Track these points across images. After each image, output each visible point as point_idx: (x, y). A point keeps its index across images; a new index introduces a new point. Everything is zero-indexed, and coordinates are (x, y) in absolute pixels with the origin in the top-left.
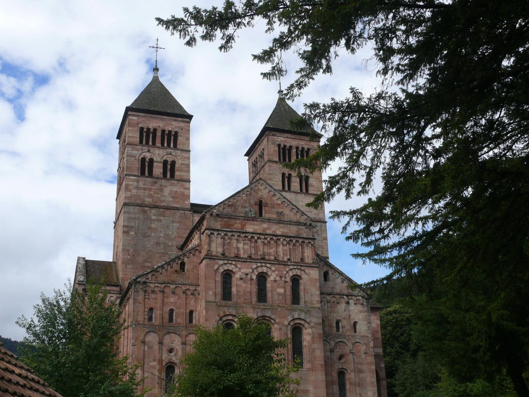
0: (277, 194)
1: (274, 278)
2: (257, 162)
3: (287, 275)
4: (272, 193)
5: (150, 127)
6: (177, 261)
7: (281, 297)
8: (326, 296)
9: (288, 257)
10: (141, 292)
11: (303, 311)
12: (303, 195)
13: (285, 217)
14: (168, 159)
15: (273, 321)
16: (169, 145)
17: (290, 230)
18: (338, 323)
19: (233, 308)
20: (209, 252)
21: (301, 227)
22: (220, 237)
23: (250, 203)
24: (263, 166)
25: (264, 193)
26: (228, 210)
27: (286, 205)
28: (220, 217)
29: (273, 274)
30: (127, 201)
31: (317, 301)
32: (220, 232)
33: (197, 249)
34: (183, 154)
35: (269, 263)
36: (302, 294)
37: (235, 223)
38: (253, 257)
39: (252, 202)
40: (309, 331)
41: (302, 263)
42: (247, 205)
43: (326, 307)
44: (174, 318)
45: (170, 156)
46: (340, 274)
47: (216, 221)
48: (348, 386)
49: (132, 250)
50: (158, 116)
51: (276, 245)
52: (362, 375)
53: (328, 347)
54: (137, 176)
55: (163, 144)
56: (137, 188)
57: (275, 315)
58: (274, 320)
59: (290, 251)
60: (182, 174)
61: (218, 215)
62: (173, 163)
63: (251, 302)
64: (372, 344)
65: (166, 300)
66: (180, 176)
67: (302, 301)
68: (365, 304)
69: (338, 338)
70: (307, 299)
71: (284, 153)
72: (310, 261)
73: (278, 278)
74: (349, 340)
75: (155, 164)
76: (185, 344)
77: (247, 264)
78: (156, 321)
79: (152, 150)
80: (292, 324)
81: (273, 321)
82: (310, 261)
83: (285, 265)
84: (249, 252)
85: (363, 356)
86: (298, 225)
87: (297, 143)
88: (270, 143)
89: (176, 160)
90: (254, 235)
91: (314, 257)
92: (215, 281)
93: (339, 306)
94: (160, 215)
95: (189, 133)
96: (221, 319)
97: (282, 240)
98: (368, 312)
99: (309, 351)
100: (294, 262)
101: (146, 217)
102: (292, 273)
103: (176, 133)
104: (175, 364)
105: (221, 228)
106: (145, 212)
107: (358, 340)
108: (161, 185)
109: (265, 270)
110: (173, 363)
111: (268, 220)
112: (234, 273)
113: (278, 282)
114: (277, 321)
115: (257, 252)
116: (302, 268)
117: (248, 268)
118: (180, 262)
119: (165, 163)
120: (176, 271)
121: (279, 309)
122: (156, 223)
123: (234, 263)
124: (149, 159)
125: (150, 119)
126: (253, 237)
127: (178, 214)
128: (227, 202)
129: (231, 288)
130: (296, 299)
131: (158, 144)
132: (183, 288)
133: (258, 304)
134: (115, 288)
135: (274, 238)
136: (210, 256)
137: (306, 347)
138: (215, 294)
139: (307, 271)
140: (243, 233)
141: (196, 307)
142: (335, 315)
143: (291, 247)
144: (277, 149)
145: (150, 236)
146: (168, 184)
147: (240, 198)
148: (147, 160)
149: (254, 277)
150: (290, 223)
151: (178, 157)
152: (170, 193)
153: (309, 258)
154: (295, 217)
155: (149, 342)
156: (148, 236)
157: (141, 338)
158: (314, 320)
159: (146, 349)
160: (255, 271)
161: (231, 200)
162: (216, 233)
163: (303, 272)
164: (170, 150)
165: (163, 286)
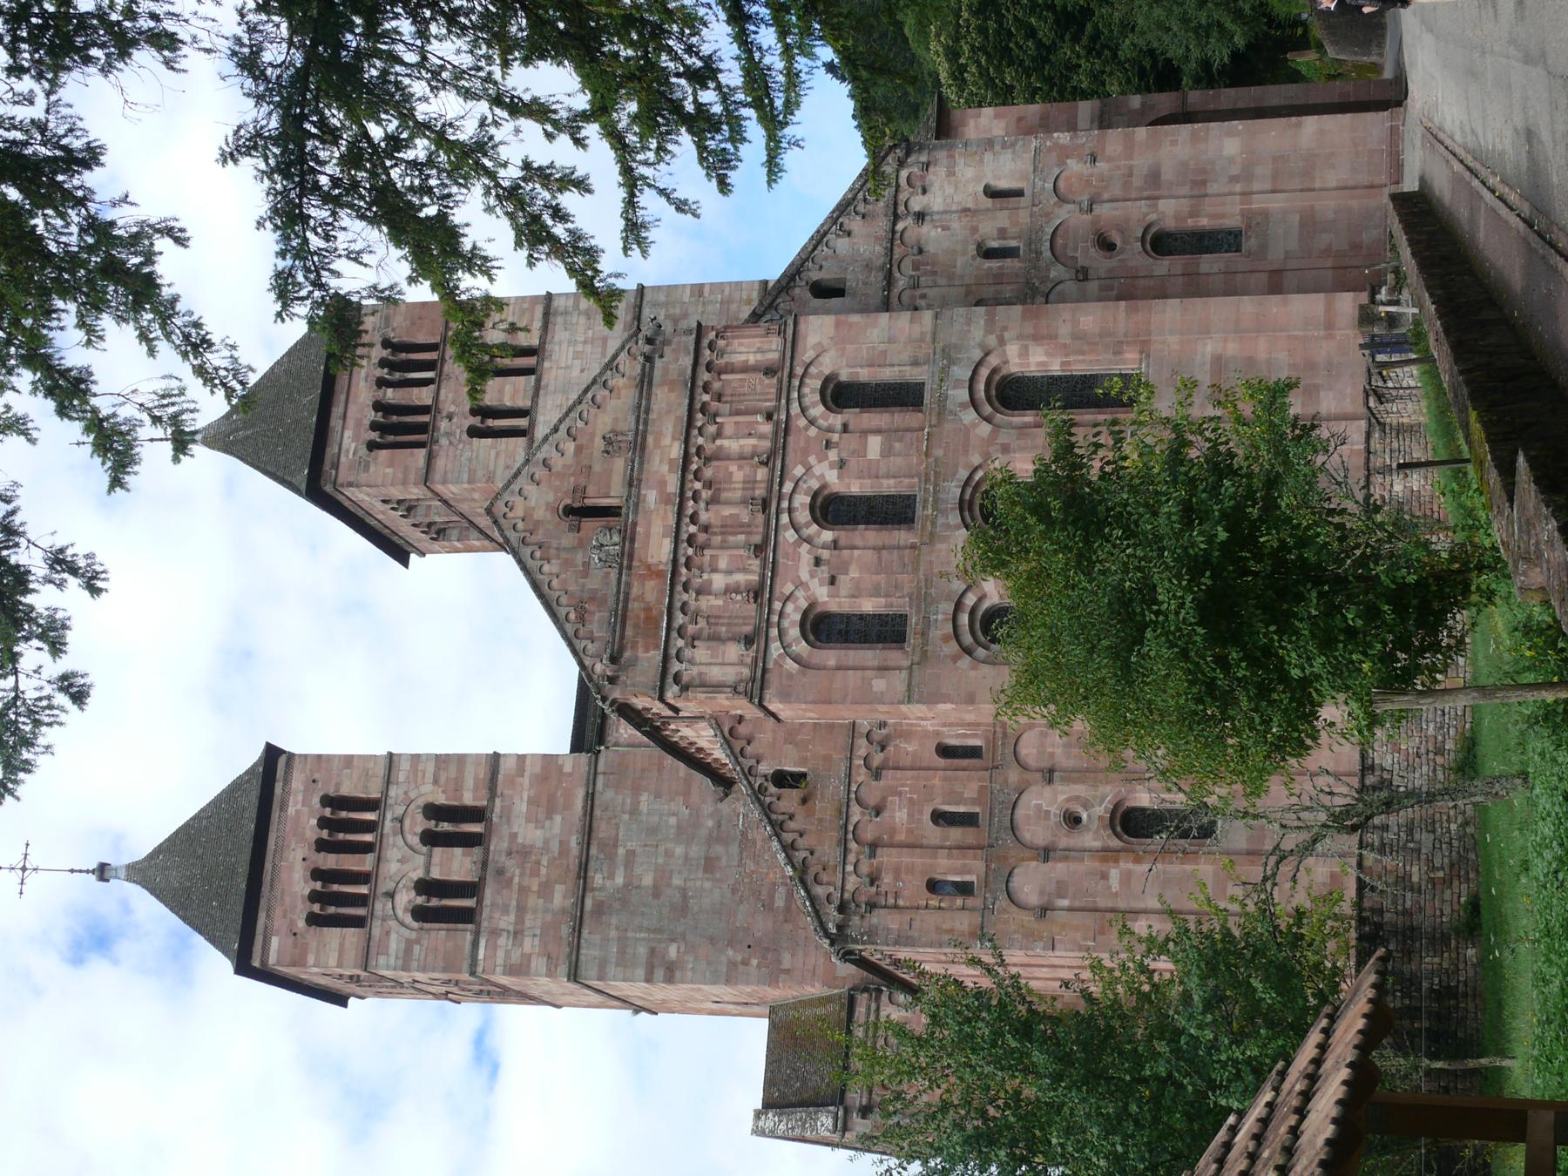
0: (540, 456)
1: (831, 467)
2: (430, 525)
3: (821, 422)
4: (540, 473)
5: (307, 892)
6: (768, 800)
7: (897, 445)
8: (896, 291)
9: (759, 418)
10: (875, 920)
11: (945, 370)
12: (546, 364)
13: (622, 426)
14: (419, 830)
15: (979, 475)
16: (369, 827)
17: (668, 412)
18: (989, 254)
19: (933, 608)
20: (741, 688)
21: (657, 373)
22: (687, 653)
23: (573, 549)
24: (445, 502)
25: (538, 501)
26: (598, 623)
27: (580, 424)
28: (621, 649)
29: (817, 471)
30: (563, 969)
31: (912, 321)
32: (673, 652)
33: (731, 730)
34: (401, 778)
35: (781, 485)
36: (887, 374)
37: (641, 598)
38: (757, 539)
39: (569, 539)
40: (1012, 350)
41: (784, 374)
42: (579, 557)
43: (931, 293)
44: (962, 809)
45: (407, 823)
46: (819, 242)
47: (634, 662)
48: (1204, 223)
49: (730, 952)
50: (268, 866)
51: (718, 459)
52: (1167, 174)
53: (1070, 287)
54: (477, 935)
55: (366, 848)
56: (517, 934)
57: (956, 466)
58: (975, 470)
59: (738, 413)
60: (469, 782)
61: (614, 659)
62: (434, 812)
63: (913, 547)
64: (1063, 138)
65: (901, 837)
66: (476, 789)
68: (924, 158)
69: (1039, 253)
70: (905, 357)
71: (400, 428)
72: (775, 343)
73: (833, 455)
74: (1047, 215)
75: (436, 874)
76: (1051, 771)
77: (781, 560)
78: (971, 870)
79: (385, 885)
80: (988, 409)
81: (979, 475)
82: (775, 343)
83: (787, 431)
84: (742, 552)
85: (1102, 165)
87: (362, 383)
88: (363, 477)
89: (421, 802)
90: (685, 536)
91: (760, 331)
93: (931, 248)
94: (611, 857)
95: (329, 758)
96: (968, 651)
97: (700, 441)
98: (951, 148)
99: (1082, 353)
100: (779, 400)
101: (617, 905)
102: (814, 405)
103: (327, 801)
104: (1117, 806)
105: (657, 647)
106: (600, 909)
108: (509, 854)
109: (802, 500)
110: (1113, 813)
111: (630, 485)
112: (812, 606)
113: (844, 455)
114: (976, 460)
115: (742, 526)
116: (799, 371)
117: (797, 558)
118: (772, 789)
119: (431, 839)
120: (804, 801)
121: (938, 452)
122: (638, 870)
123: (777, 605)
124: (419, 893)
125: (278, 894)
126: (691, 540)
127: (610, 794)
128: (569, 628)
129: (862, 617)
130: (904, 396)
131: (365, 863)
132: (860, 779)
133: (918, 525)
134: (860, 1011)
135: (694, 467)
136: (755, 687)
137: (1068, 363)
138: (883, 669)
139: (809, 355)
141: (926, 734)
143: (725, 408)
144: (384, 452)
145: (683, 891)
146: (505, 831)
147: (555, 583)
148: (420, 900)
149: (827, 536)
150: (642, 411)
151: (412, 795)
152: (537, 821)
153: (766, 347)
154: (623, 392)
155: (1042, 893)
156: (685, 897)
157: (1027, 918)
158: (977, 333)
159: (1065, 903)
160: (806, 532)
161: (562, 612)
162: (675, 667)
163: (813, 370)
164: (388, 824)
165: (853, 845)
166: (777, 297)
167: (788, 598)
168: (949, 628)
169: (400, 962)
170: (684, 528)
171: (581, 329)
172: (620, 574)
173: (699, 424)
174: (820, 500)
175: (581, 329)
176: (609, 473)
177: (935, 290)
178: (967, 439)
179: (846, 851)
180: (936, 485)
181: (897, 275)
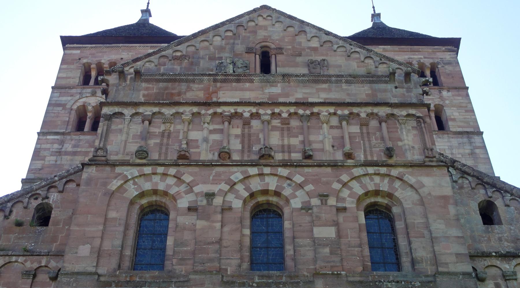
5: (103, 61)
7: (327, 250)
8: (498, 263)
9: (348, 147)
17: (348, 95)
21: (382, 86)
22: (139, 119)
23: (232, 50)
27: (335, 47)
28: (147, 81)
29: (299, 193)
30: (32, 176)
31: (458, 255)
32: (141, 110)
37: (189, 89)
38: (236, 157)
39: (240, 48)
50: (121, 45)
54: (63, 134)
59: (351, 137)
63: (220, 271)
70: (421, 252)
73: (315, 202)
86: (371, 82)
87: (407, 57)
92: (106, 219)
102: (363, 186)
109: (272, 184)
113: (315, 210)
115: (250, 147)
116: (395, 172)
117: (216, 182)
118: (34, 204)
123: (172, 171)
125: (105, 50)
135: (301, 112)
138: (99, 254)
143: (355, 129)
147: (206, 44)
148: (90, 108)
149: (237, 204)
160: (240, 187)
162: (128, 112)
163: (397, 184)
166: (473, 176)
167: (179, 179)
169: (53, 102)
171: (461, 151)
173: (339, 112)
174: (274, 199)
175: (461, 151)
176: (296, 65)
181: (514, 262)
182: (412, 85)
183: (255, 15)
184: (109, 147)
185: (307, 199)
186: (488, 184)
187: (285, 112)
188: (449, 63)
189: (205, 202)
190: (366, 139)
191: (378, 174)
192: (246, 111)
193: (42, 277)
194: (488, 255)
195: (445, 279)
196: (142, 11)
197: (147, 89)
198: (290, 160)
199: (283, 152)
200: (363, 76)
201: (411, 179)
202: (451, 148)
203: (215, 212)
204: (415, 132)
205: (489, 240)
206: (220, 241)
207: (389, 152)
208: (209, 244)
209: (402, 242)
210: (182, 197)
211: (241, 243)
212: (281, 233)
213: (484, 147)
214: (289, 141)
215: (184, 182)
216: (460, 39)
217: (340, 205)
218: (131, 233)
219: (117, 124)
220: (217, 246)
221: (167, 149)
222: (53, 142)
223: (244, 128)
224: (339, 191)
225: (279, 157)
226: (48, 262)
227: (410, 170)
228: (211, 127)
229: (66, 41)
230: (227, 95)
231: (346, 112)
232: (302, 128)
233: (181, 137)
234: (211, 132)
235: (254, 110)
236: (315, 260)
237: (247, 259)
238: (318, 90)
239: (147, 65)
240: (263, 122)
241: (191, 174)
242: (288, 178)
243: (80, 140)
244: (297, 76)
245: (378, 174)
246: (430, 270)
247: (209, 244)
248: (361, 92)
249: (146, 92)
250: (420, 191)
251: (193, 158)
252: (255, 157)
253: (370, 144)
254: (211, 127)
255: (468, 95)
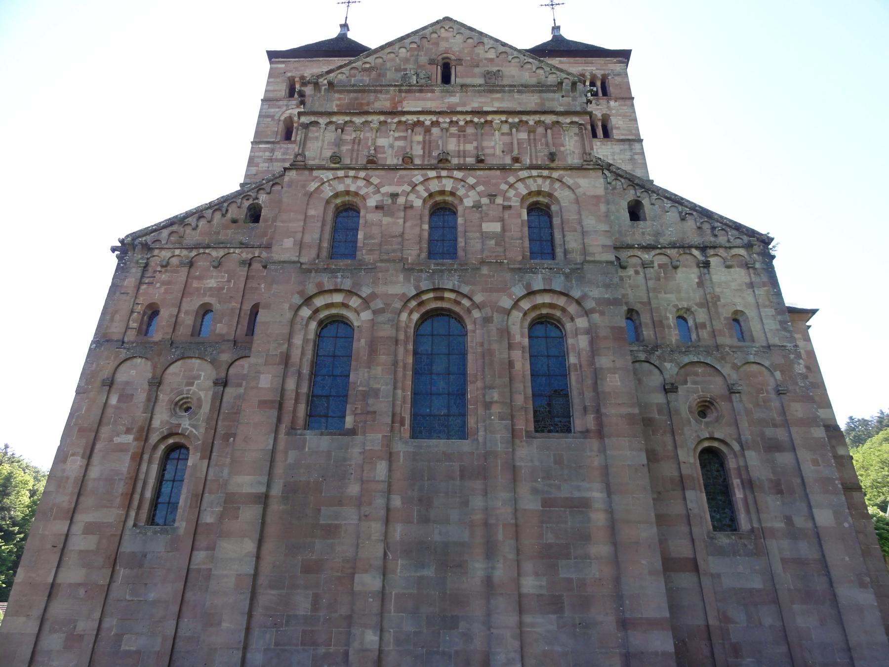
7: (493, 242)
8: (639, 253)
9: (516, 152)
15: (466, 302)
17: (519, 103)
20: (299, 158)
21: (551, 95)
22: (332, 128)
23: (416, 61)
27: (510, 57)
28: (340, 92)
29: (472, 193)
30: (248, 181)
31: (604, 246)
32: (334, 119)
37: (377, 99)
38: (417, 161)
39: (423, 60)
40: (582, 323)
52: (784, 459)
53: (656, 380)
54: (273, 143)
58: (470, 299)
63: (402, 260)
65: (195, 284)
67: (559, 251)
69: (686, 352)
70: (573, 243)
73: (485, 200)
80: (526, 305)
86: (540, 92)
87: (580, 68)
92: (306, 216)
93: (680, 274)
102: (527, 187)
107: (751, 358)
109: (448, 185)
110: (182, 434)
113: (484, 208)
115: (430, 152)
116: (555, 175)
117: (399, 184)
118: (247, 204)
121: (485, 270)
123: (362, 174)
125: (307, 64)
135: (476, 120)
138: (301, 245)
140: (392, 113)
142: (672, 297)
143: (523, 135)
147: (392, 55)
149: (418, 203)
157: (106, 373)
158: (596, 293)
159: (114, 400)
160: (420, 188)
162: (323, 121)
163: (557, 185)
165: (194, 253)
166: (625, 178)
167: (368, 181)
168: (328, 286)
170: (428, 117)
171: (622, 157)
172: (395, 86)
173: (510, 120)
174: (449, 199)
175: (622, 157)
176: (474, 76)
177: (643, 281)
178: (498, 290)
179: (190, 249)
180: (456, 270)
181: (653, 253)
182: (577, 94)
183: (438, 26)
184: (307, 153)
185: (478, 198)
186: (637, 185)
187: (461, 120)
188: (618, 75)
189: (390, 201)
190: (533, 145)
191: (541, 176)
192: (427, 120)
193: (256, 266)
194: (631, 247)
195: (591, 266)
196: (341, 26)
197: (340, 99)
198: (465, 164)
199: (459, 157)
200: (533, 86)
201: (569, 181)
202: (613, 154)
203: (399, 210)
204: (576, 138)
205: (634, 234)
206: (402, 235)
207: (552, 157)
208: (393, 237)
209: (558, 236)
210: (370, 197)
211: (420, 236)
212: (455, 228)
213: (643, 153)
214: (464, 146)
215: (372, 184)
216: (630, 51)
217: (506, 203)
218: (328, 228)
219: (313, 132)
220: (400, 239)
221: (358, 154)
222: (265, 150)
223: (425, 135)
224: (506, 192)
225: (455, 161)
226: (261, 253)
227: (569, 172)
228: (397, 135)
229: (273, 55)
230: (410, 105)
231: (517, 120)
232: (476, 134)
233: (370, 144)
234: (396, 139)
235: (434, 119)
236: (482, 250)
237: (425, 250)
238: (493, 100)
239: (340, 76)
240: (442, 130)
241: (378, 177)
242: (462, 180)
243: (288, 149)
244: (474, 86)
245: (541, 176)
246: (579, 259)
247: (393, 237)
248: (531, 101)
249: (338, 103)
250: (577, 191)
251: (381, 162)
252: (434, 162)
253: (536, 149)
254: (397, 135)
255: (633, 105)
